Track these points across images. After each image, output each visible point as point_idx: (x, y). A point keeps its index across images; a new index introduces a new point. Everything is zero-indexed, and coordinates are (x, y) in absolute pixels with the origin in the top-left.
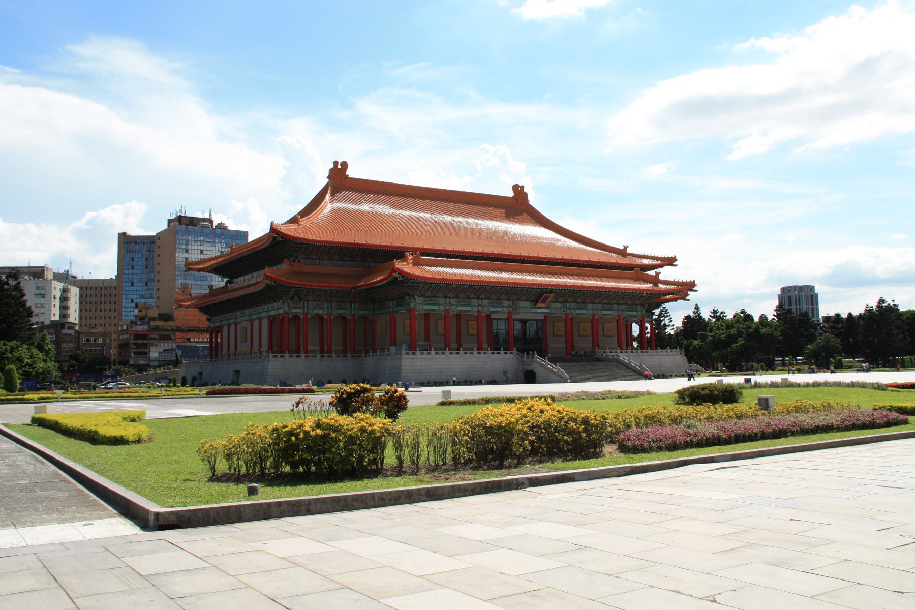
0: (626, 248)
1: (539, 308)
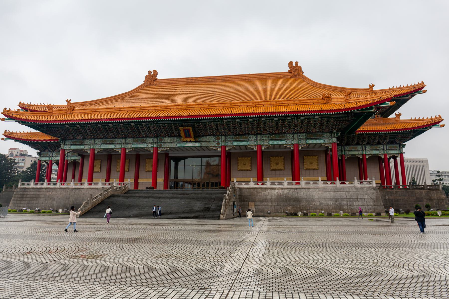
1: (187, 142)
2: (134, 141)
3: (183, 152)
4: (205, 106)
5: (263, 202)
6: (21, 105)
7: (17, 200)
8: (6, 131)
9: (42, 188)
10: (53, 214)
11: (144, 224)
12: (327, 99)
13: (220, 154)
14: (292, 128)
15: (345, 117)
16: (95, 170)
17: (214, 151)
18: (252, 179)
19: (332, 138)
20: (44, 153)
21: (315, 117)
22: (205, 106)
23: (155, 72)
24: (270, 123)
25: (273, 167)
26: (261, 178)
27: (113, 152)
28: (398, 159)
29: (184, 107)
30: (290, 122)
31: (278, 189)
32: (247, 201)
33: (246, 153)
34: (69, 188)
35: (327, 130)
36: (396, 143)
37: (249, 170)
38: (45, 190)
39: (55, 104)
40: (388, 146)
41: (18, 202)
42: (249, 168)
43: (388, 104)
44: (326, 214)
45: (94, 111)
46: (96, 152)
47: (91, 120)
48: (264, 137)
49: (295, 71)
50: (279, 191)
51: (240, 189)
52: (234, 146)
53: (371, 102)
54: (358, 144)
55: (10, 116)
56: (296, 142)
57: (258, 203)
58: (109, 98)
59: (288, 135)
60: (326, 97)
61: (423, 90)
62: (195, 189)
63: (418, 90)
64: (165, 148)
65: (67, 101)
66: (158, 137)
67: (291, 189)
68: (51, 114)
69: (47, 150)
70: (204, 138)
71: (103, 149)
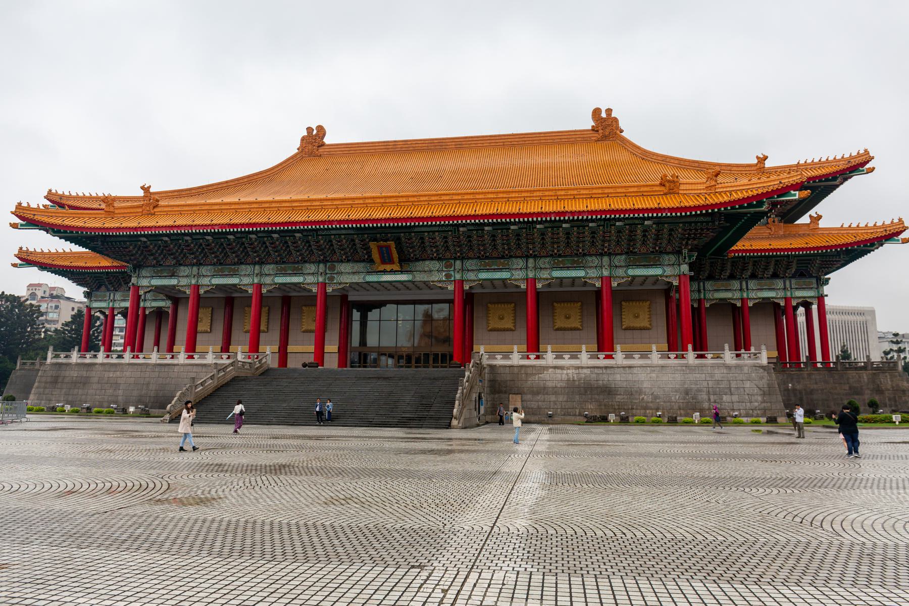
0: (762, 160)
1: (385, 272)
2: (278, 270)
3: (377, 292)
4: (422, 199)
5: (538, 393)
6: (50, 196)
7: (45, 388)
8: (21, 248)
9: (96, 364)
10: (117, 415)
11: (299, 437)
12: (670, 186)
13: (451, 297)
14: (599, 244)
15: (707, 222)
16: (199, 329)
17: (440, 291)
18: (515, 348)
19: (679, 265)
20: (98, 293)
21: (646, 223)
22: (422, 199)
23: (321, 129)
24: (553, 234)
25: (559, 324)
26: (534, 346)
27: (236, 291)
28: (815, 307)
29: (378, 201)
30: (593, 233)
31: (568, 368)
32: (505, 392)
33: (504, 296)
34: (147, 365)
35: (669, 249)
36: (811, 276)
37: (511, 330)
38: (101, 368)
39: (119, 195)
40: (793, 281)
41: (47, 391)
42: (511, 326)
43: (795, 195)
44: (666, 420)
45: (198, 208)
46: (202, 291)
47: (191, 226)
48: (542, 262)
49: (606, 127)
50: (570, 371)
51: (492, 367)
52: (480, 280)
53: (760, 191)
54: (732, 277)
55: (28, 218)
56: (606, 273)
57: (529, 397)
58: (227, 182)
59: (589, 259)
60: (669, 181)
61: (867, 166)
62: (402, 367)
63: (857, 166)
64: (340, 284)
65: (142, 188)
66: (327, 261)
67: (594, 367)
68: (111, 214)
69: (103, 288)
70: (420, 265)
71: (217, 285)
